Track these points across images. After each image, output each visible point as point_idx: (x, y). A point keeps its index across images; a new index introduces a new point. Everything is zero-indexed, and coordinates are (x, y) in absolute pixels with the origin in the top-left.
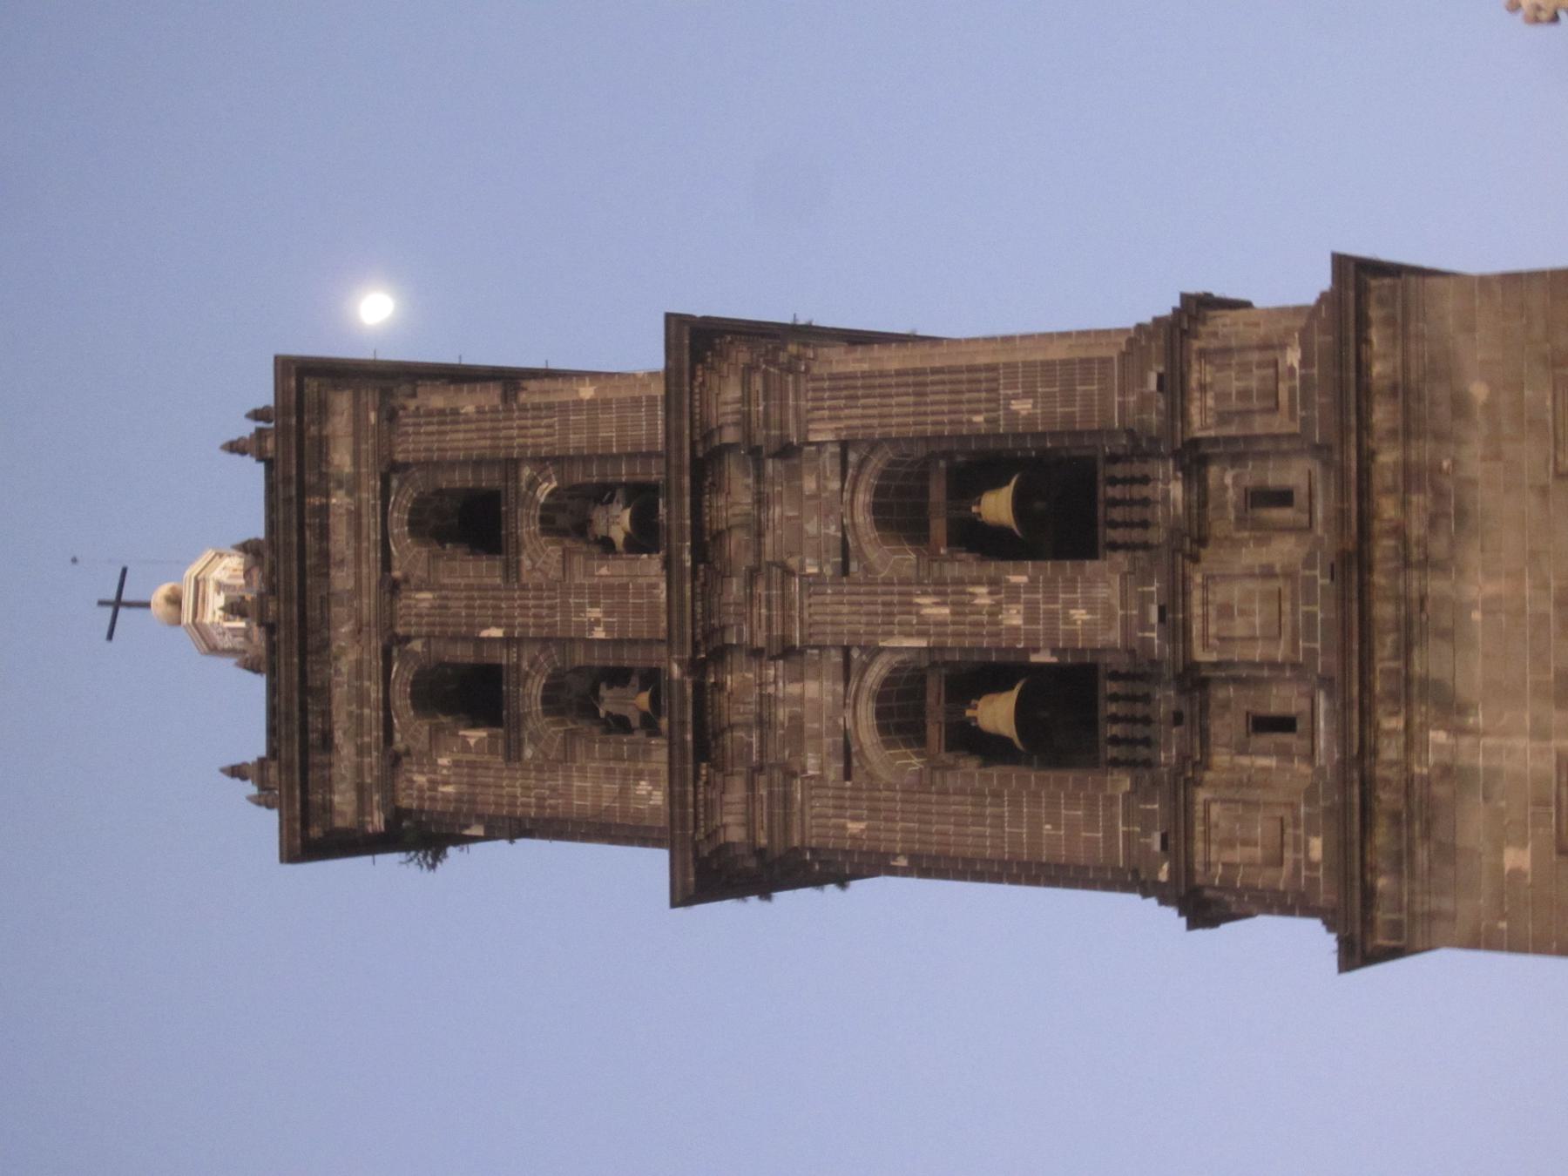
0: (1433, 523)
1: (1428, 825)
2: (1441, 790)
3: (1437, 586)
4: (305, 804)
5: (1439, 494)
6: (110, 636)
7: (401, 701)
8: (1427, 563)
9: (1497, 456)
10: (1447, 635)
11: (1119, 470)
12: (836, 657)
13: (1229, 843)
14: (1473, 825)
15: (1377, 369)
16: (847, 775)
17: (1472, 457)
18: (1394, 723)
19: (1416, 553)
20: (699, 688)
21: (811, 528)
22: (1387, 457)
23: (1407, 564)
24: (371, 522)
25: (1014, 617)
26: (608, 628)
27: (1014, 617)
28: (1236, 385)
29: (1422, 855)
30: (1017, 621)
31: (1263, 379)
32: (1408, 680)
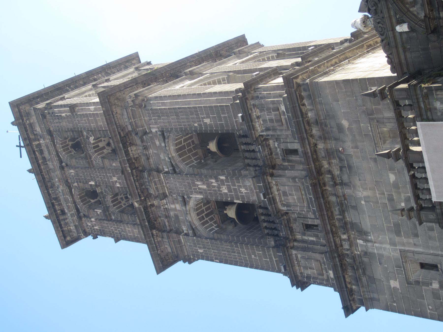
0: (341, 168)
1: (364, 270)
2: (366, 260)
3: (348, 191)
4: (63, 231)
5: (341, 160)
6: (21, 157)
7: (78, 201)
8: (342, 184)
9: (357, 147)
10: (355, 208)
11: (244, 140)
12: (180, 199)
13: (306, 268)
14: (378, 272)
15: (310, 114)
16: (195, 234)
17: (348, 146)
18: (344, 237)
19: (338, 181)
20: (146, 208)
21: (162, 156)
22: (321, 146)
23: (335, 184)
24: (52, 148)
25: (224, 190)
26: (120, 183)
27: (224, 190)
28: (268, 117)
29: (364, 279)
30: (226, 191)
31: (275, 115)
32: (346, 223)
